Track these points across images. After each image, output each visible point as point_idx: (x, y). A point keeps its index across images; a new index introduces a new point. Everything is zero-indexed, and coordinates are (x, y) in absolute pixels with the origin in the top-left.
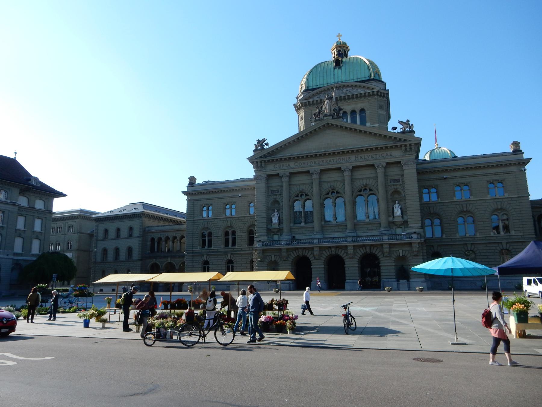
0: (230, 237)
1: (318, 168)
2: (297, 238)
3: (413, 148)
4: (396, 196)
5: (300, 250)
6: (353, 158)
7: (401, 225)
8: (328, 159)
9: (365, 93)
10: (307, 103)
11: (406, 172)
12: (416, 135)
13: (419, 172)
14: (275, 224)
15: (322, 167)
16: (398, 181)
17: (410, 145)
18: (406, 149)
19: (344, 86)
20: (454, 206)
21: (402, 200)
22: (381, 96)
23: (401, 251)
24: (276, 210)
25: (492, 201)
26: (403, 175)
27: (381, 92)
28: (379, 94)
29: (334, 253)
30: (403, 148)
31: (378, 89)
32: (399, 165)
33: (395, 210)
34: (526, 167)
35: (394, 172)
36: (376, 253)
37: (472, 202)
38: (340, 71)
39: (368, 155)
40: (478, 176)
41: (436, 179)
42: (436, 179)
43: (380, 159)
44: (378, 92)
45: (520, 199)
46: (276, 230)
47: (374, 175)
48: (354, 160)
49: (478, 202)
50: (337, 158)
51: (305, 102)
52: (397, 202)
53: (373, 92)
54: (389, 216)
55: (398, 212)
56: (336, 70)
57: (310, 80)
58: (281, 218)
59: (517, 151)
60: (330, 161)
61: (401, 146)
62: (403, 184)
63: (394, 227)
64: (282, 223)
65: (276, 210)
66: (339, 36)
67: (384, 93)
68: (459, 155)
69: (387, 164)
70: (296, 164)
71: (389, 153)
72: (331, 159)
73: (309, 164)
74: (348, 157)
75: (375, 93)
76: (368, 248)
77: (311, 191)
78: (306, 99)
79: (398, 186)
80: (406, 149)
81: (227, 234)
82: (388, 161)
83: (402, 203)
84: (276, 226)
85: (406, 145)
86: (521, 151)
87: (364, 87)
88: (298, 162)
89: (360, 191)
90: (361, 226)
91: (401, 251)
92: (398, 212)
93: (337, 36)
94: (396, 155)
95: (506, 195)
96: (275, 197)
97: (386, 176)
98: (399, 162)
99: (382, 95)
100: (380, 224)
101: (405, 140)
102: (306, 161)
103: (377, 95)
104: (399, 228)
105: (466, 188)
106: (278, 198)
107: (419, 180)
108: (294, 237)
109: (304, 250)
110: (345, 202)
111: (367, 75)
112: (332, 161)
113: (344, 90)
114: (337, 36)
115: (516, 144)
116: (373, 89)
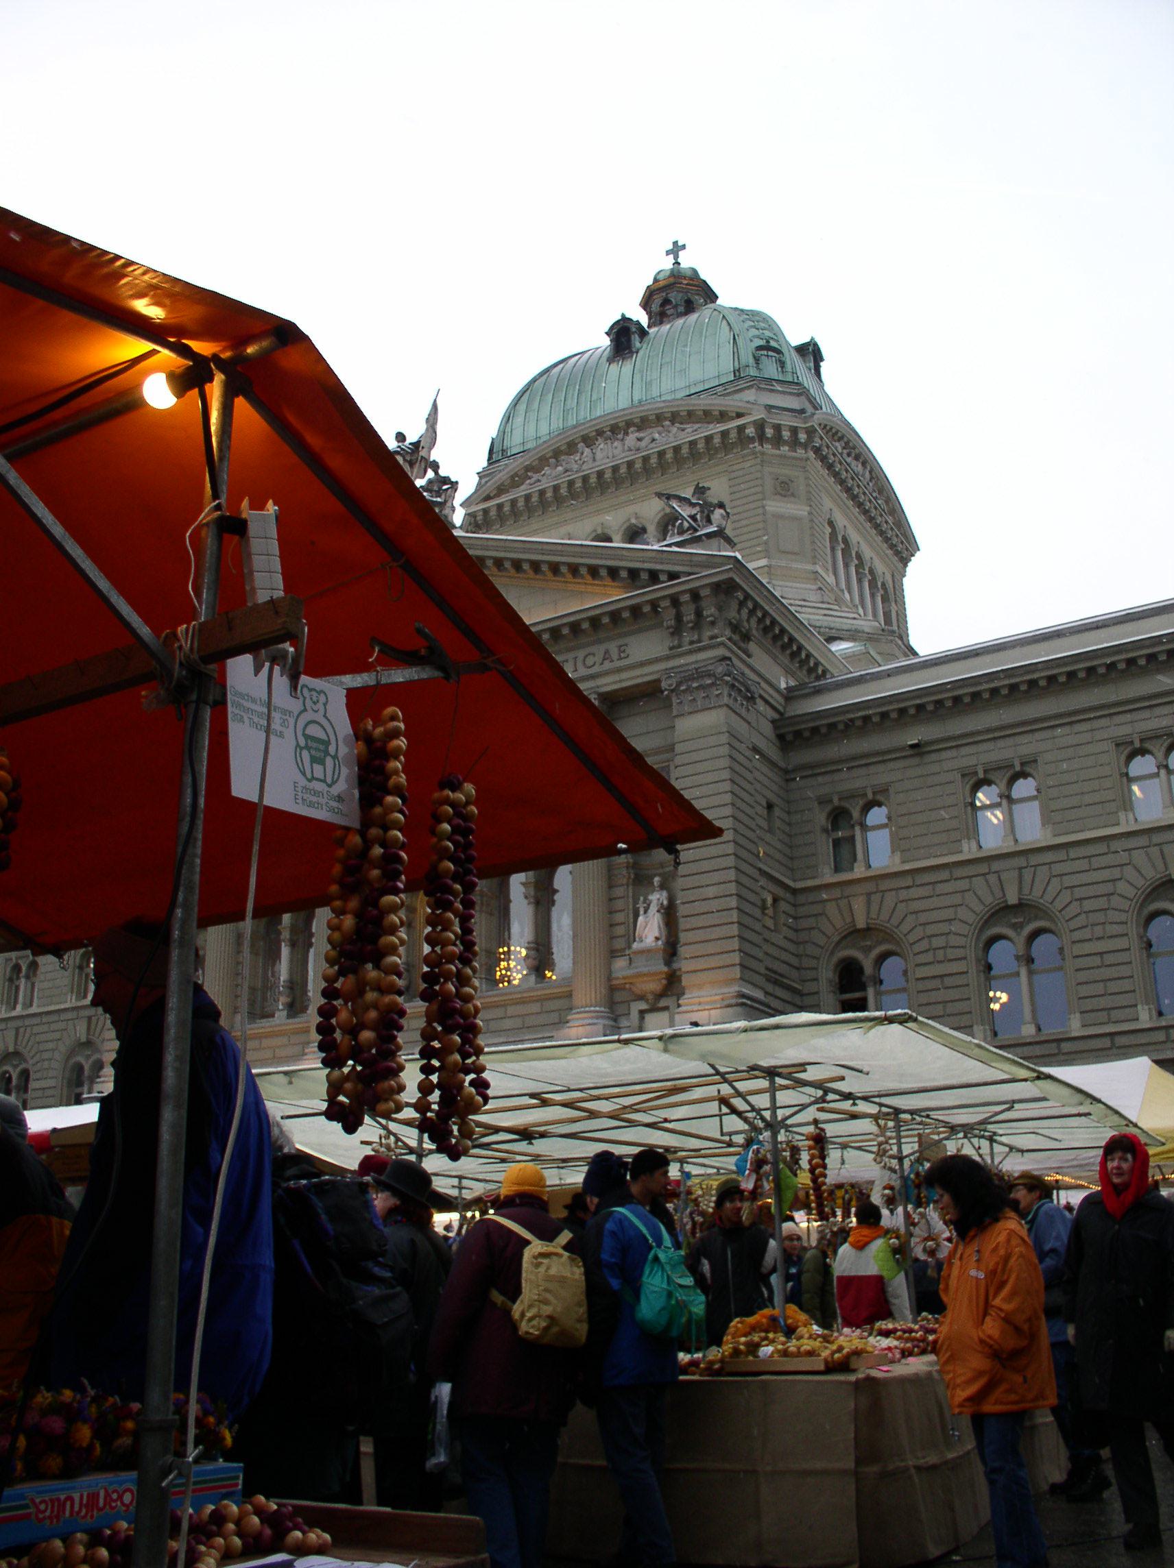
3: (710, 611)
7: (662, 995)
9: (709, 439)
10: (493, 513)
17: (695, 595)
18: (679, 618)
19: (629, 424)
20: (963, 884)
22: (778, 440)
27: (777, 428)
28: (769, 432)
30: (669, 618)
31: (758, 415)
33: (641, 919)
38: (627, 367)
40: (1071, 718)
42: (882, 757)
44: (760, 426)
49: (1073, 853)
51: (486, 511)
53: (741, 429)
54: (613, 954)
56: (614, 368)
57: (519, 420)
61: (654, 604)
66: (676, 249)
67: (794, 431)
71: (613, 647)
75: (750, 431)
78: (488, 498)
80: (679, 618)
85: (675, 601)
87: (707, 413)
90: (498, 1013)
93: (668, 253)
99: (786, 434)
101: (673, 576)
103: (761, 437)
104: (654, 1009)
111: (727, 365)
113: (631, 439)
114: (668, 253)
116: (739, 415)
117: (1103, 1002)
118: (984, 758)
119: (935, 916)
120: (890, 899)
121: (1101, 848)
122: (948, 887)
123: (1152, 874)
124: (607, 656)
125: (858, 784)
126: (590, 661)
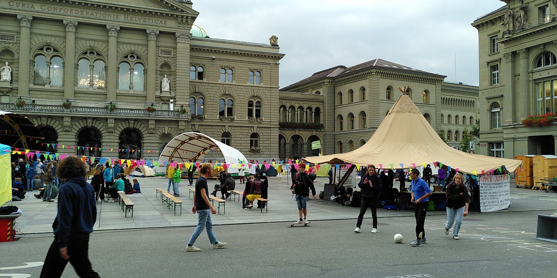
0: (254, 108)
1: (75, 20)
2: (37, 103)
4: (165, 69)
5: (43, 119)
6: (121, 17)
8: (90, 12)
11: (179, 45)
12: (194, 7)
13: (193, 49)
14: (5, 81)
15: (81, 20)
16: (169, 53)
17: (187, 17)
18: (182, 20)
20: (218, 88)
21: (172, 74)
23: (166, 128)
24: (7, 63)
25: (251, 88)
26: (175, 48)
29: (90, 125)
32: (172, 37)
34: (280, 61)
35: (166, 42)
36: (140, 129)
37: (234, 87)
39: (140, 18)
40: (241, 61)
41: (205, 58)
42: (205, 58)
43: (153, 25)
45: (272, 89)
46: (7, 90)
47: (144, 42)
48: (122, 20)
49: (239, 87)
50: (102, 13)
52: (166, 76)
55: (166, 86)
58: (14, 75)
59: (275, 45)
60: (92, 14)
61: (177, 16)
62: (175, 57)
63: (161, 103)
64: (17, 81)
65: (7, 63)
68: (212, 36)
69: (161, 32)
70: (44, 7)
71: (163, 20)
72: (94, 12)
73: (62, 12)
74: (116, 14)
76: (132, 122)
77: (62, 46)
79: (169, 59)
80: (182, 20)
81: (250, 104)
82: (162, 29)
83: (172, 77)
84: (8, 85)
85: (182, 16)
86: (278, 46)
88: (47, 6)
89: (126, 57)
91: (166, 128)
92: (166, 86)
94: (170, 25)
95: (262, 85)
96: (7, 45)
97: (157, 46)
98: (174, 34)
100: (146, 97)
101: (182, 11)
102: (58, 7)
105: (230, 72)
106: (12, 47)
107: (191, 57)
108: (34, 101)
109: (50, 119)
110: (106, 68)
112: (95, 15)
115: (274, 39)
117: (241, 115)
118: (225, 64)
119: (212, 93)
120: (203, 87)
121: (244, 87)
122: (216, 88)
123: (252, 95)
124: (161, 22)
125: (200, 62)
126: (157, 22)
